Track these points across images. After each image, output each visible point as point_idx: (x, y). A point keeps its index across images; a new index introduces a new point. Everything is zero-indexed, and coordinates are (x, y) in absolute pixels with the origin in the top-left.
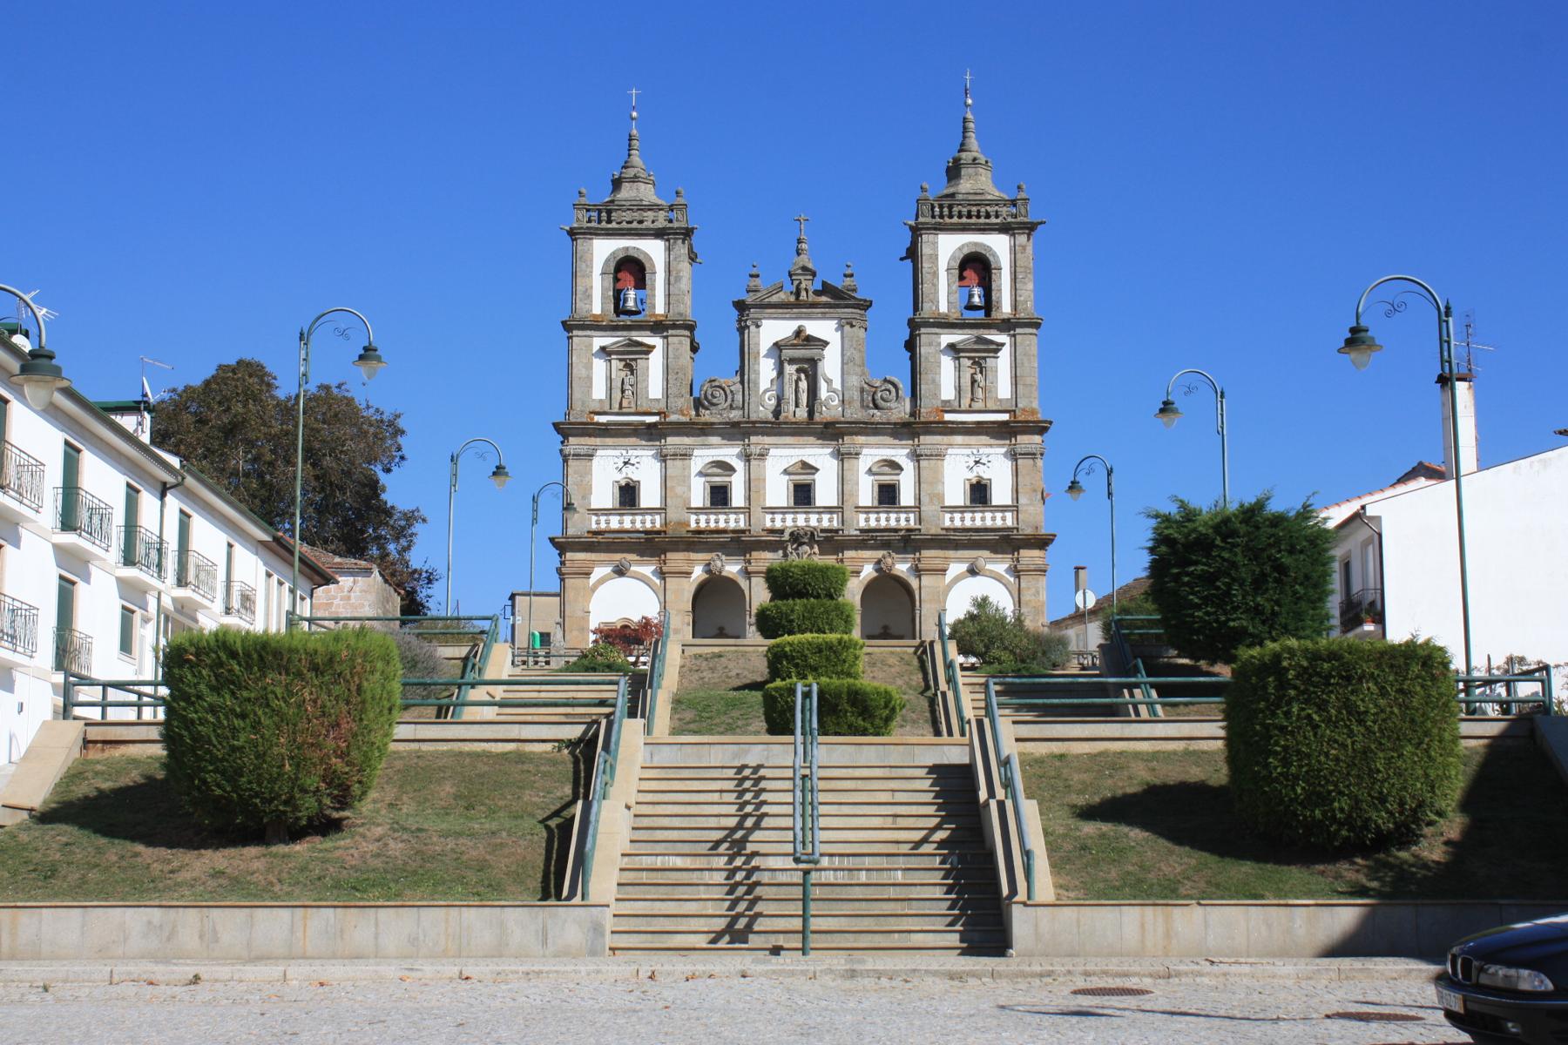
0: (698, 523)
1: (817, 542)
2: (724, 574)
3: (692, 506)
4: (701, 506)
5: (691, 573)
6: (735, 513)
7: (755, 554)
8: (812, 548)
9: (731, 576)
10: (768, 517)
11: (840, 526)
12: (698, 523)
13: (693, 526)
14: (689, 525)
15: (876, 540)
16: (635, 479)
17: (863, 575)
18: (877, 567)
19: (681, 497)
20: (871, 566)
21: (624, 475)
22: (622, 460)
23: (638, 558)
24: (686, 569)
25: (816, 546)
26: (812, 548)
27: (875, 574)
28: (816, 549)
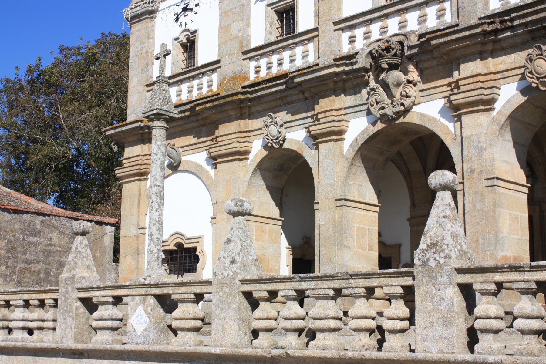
0: (257, 72)
1: (410, 58)
2: (286, 146)
3: (253, 45)
4: (261, 43)
5: (247, 153)
6: (301, 43)
7: (324, 104)
8: (406, 72)
9: (295, 148)
10: (346, 36)
11: (456, 21)
12: (257, 72)
13: (252, 77)
14: (248, 79)
15: (512, 28)
16: (192, 29)
17: (498, 106)
18: (524, 84)
19: (236, 37)
20: (516, 84)
21: (183, 27)
22: (182, 6)
23: (195, 140)
24: (242, 147)
25: (411, 67)
26: (406, 72)
27: (522, 99)
28: (414, 75)
